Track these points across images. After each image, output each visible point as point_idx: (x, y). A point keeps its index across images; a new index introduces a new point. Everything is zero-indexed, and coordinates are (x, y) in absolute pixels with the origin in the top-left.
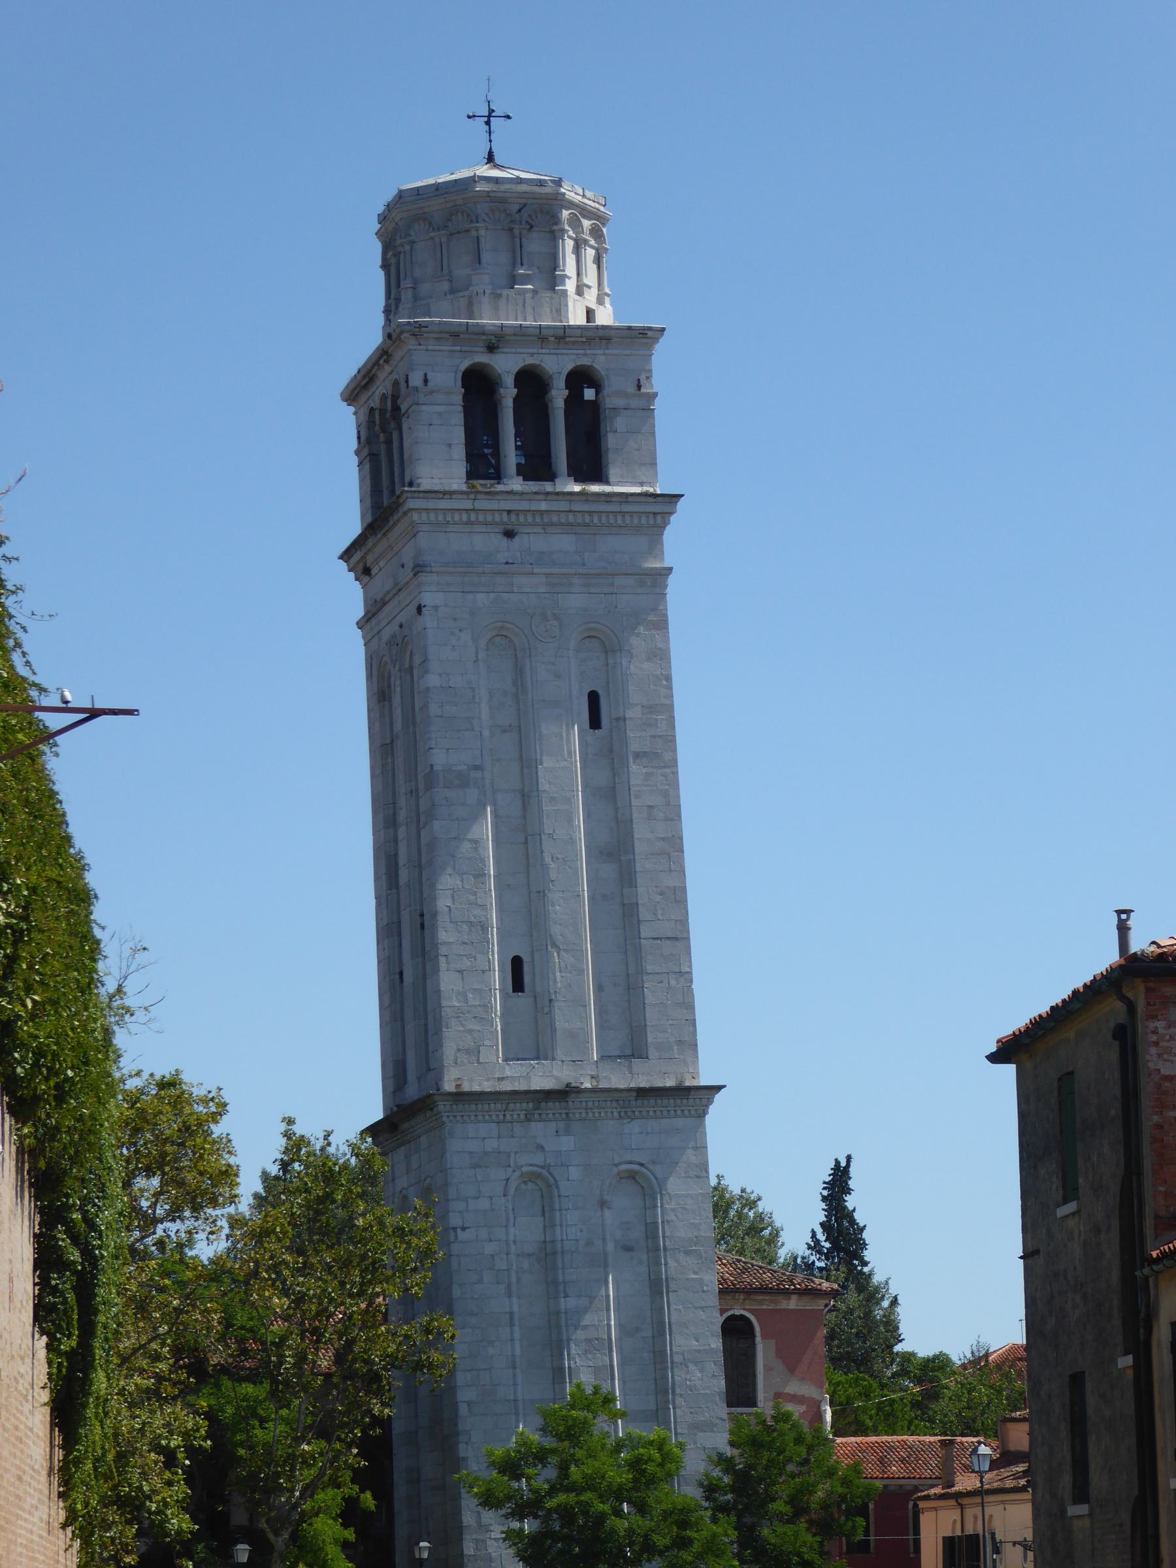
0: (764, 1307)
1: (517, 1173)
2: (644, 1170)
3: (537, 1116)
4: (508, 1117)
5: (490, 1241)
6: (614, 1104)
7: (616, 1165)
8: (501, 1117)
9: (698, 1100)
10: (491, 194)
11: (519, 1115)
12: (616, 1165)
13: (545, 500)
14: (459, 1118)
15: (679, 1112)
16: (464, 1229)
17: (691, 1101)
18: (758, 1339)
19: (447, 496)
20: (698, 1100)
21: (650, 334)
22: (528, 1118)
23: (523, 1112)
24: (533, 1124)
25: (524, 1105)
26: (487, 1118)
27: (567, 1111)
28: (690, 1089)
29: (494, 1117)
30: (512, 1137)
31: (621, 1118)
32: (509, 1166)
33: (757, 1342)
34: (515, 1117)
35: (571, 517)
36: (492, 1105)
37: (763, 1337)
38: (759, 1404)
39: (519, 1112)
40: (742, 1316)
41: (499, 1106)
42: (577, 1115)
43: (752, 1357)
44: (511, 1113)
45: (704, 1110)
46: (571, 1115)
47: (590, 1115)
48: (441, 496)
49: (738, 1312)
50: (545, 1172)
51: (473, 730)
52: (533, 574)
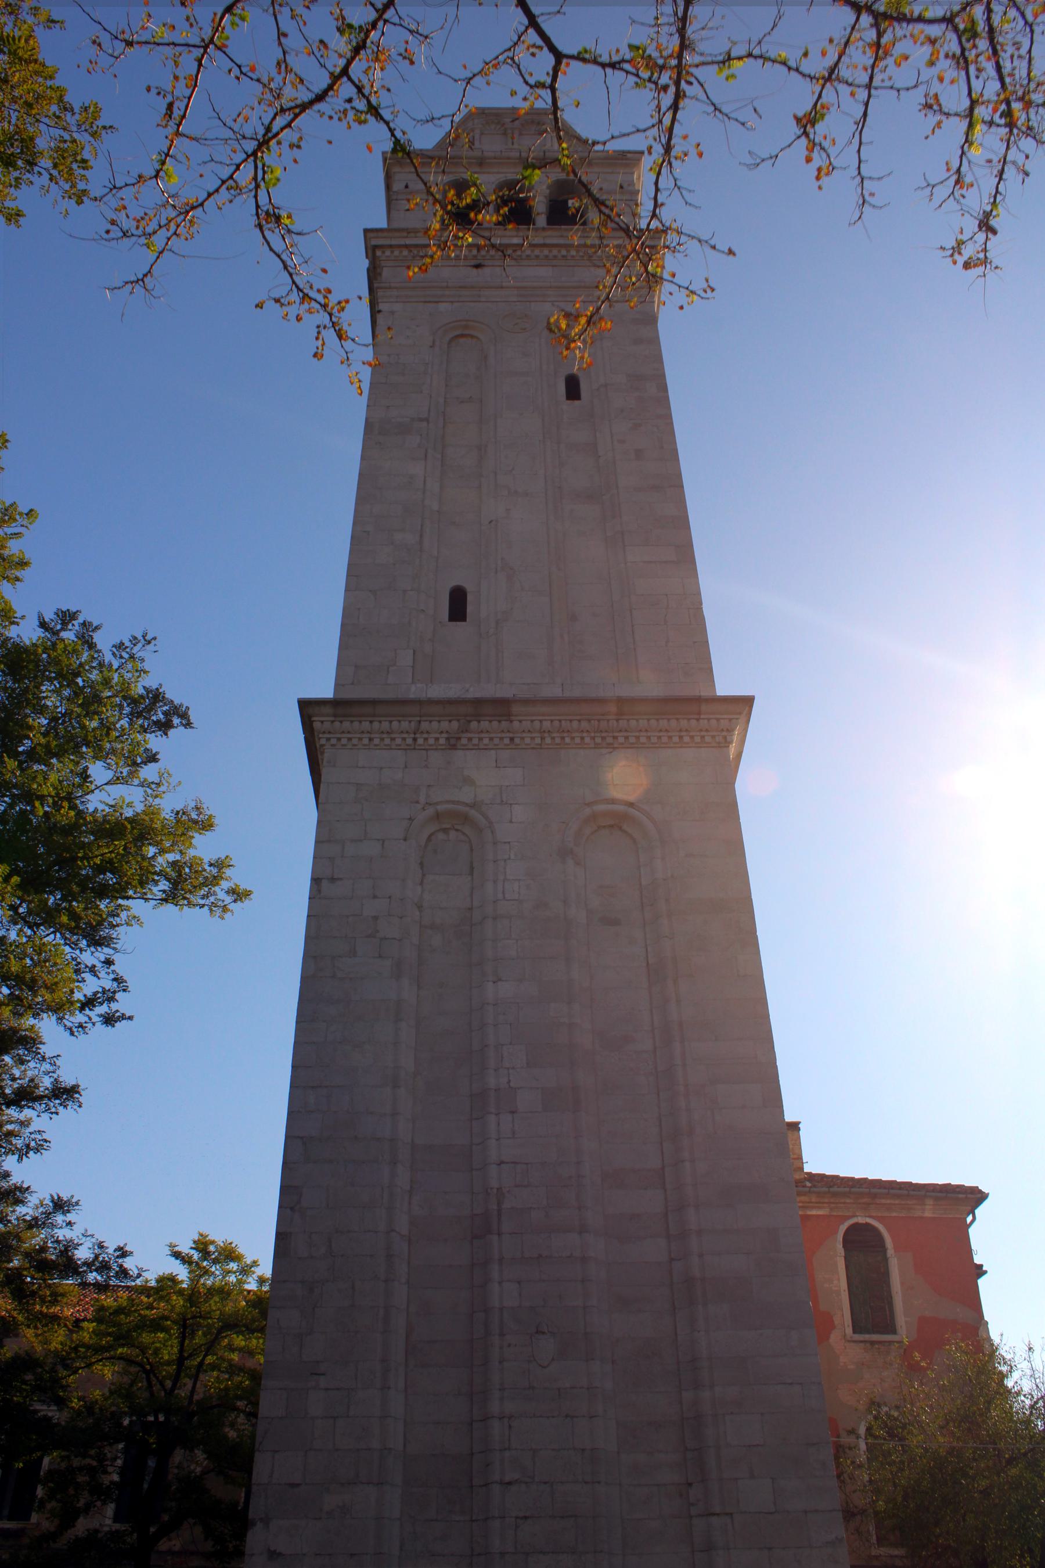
0: (894, 1214)
1: (430, 811)
2: (631, 811)
3: (464, 741)
4: (420, 741)
5: (375, 897)
6: (585, 725)
7: (589, 805)
8: (409, 741)
9: (714, 722)
10: (486, 111)
11: (437, 739)
12: (589, 805)
13: (517, 236)
14: (344, 741)
15: (686, 739)
16: (333, 880)
17: (704, 723)
18: (890, 1251)
19: (412, 235)
20: (714, 722)
21: (629, 155)
22: (453, 744)
23: (445, 735)
24: (460, 753)
25: (445, 725)
26: (387, 741)
27: (511, 735)
28: (699, 700)
29: (398, 741)
30: (426, 767)
31: (597, 746)
32: (417, 802)
33: (889, 1255)
34: (431, 741)
35: (546, 252)
36: (395, 724)
37: (897, 1249)
38: (899, 1330)
39: (437, 735)
40: (867, 1224)
41: (405, 725)
42: (528, 741)
43: (884, 1276)
44: (425, 736)
45: (725, 738)
46: (517, 741)
47: (548, 740)
48: (405, 234)
49: (861, 1220)
50: (473, 813)
51: (421, 392)
52: (502, 287)
